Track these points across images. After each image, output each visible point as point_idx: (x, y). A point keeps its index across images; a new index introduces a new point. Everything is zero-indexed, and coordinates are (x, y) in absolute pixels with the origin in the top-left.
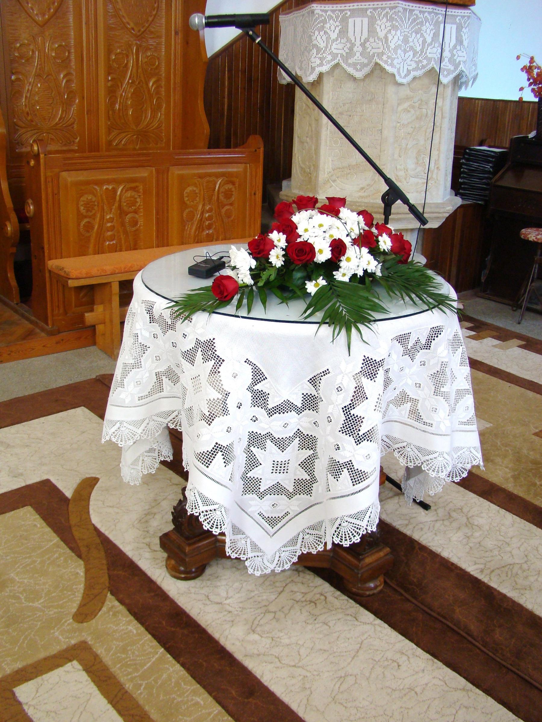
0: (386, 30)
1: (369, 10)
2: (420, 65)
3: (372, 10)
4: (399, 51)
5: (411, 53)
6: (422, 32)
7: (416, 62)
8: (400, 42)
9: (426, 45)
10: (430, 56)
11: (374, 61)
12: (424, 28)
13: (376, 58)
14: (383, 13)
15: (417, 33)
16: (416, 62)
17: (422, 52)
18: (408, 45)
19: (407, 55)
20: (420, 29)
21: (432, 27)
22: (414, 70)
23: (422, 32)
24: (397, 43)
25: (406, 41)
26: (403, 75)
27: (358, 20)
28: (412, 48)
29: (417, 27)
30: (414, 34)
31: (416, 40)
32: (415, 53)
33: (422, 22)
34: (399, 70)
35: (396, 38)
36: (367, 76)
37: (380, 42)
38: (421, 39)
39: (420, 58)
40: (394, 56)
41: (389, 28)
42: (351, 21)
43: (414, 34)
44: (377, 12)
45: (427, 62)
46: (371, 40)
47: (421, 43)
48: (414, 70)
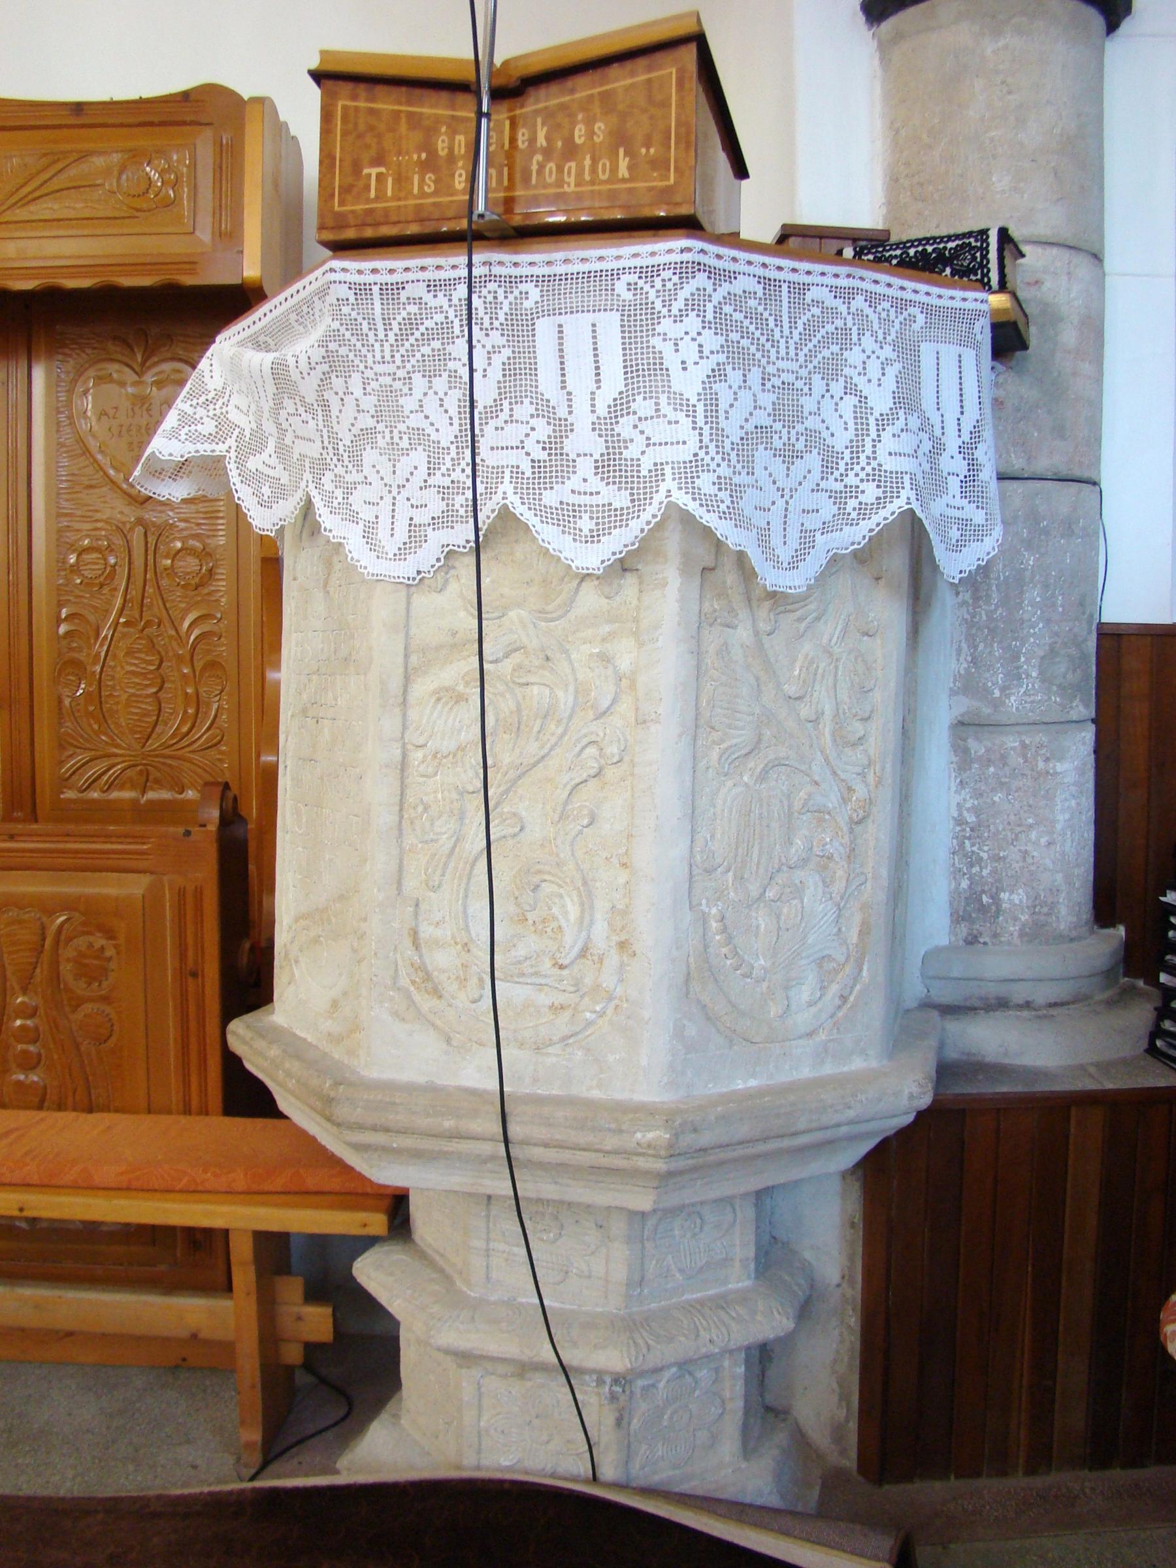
0: (706, 366)
1: (626, 278)
2: (852, 503)
3: (633, 278)
4: (762, 456)
5: (813, 460)
6: (847, 371)
8: (762, 418)
9: (872, 421)
11: (660, 497)
12: (854, 356)
13: (669, 483)
14: (683, 294)
16: (833, 495)
17: (855, 458)
18: (800, 428)
19: (799, 467)
21: (888, 352)
23: (847, 371)
24: (753, 422)
25: (787, 411)
26: (785, 554)
27: (577, 326)
32: (829, 464)
33: (846, 331)
34: (763, 539)
35: (745, 397)
36: (623, 566)
37: (681, 416)
38: (851, 400)
39: (851, 480)
40: (743, 479)
41: (714, 359)
42: (545, 328)
44: (658, 283)
46: (643, 407)
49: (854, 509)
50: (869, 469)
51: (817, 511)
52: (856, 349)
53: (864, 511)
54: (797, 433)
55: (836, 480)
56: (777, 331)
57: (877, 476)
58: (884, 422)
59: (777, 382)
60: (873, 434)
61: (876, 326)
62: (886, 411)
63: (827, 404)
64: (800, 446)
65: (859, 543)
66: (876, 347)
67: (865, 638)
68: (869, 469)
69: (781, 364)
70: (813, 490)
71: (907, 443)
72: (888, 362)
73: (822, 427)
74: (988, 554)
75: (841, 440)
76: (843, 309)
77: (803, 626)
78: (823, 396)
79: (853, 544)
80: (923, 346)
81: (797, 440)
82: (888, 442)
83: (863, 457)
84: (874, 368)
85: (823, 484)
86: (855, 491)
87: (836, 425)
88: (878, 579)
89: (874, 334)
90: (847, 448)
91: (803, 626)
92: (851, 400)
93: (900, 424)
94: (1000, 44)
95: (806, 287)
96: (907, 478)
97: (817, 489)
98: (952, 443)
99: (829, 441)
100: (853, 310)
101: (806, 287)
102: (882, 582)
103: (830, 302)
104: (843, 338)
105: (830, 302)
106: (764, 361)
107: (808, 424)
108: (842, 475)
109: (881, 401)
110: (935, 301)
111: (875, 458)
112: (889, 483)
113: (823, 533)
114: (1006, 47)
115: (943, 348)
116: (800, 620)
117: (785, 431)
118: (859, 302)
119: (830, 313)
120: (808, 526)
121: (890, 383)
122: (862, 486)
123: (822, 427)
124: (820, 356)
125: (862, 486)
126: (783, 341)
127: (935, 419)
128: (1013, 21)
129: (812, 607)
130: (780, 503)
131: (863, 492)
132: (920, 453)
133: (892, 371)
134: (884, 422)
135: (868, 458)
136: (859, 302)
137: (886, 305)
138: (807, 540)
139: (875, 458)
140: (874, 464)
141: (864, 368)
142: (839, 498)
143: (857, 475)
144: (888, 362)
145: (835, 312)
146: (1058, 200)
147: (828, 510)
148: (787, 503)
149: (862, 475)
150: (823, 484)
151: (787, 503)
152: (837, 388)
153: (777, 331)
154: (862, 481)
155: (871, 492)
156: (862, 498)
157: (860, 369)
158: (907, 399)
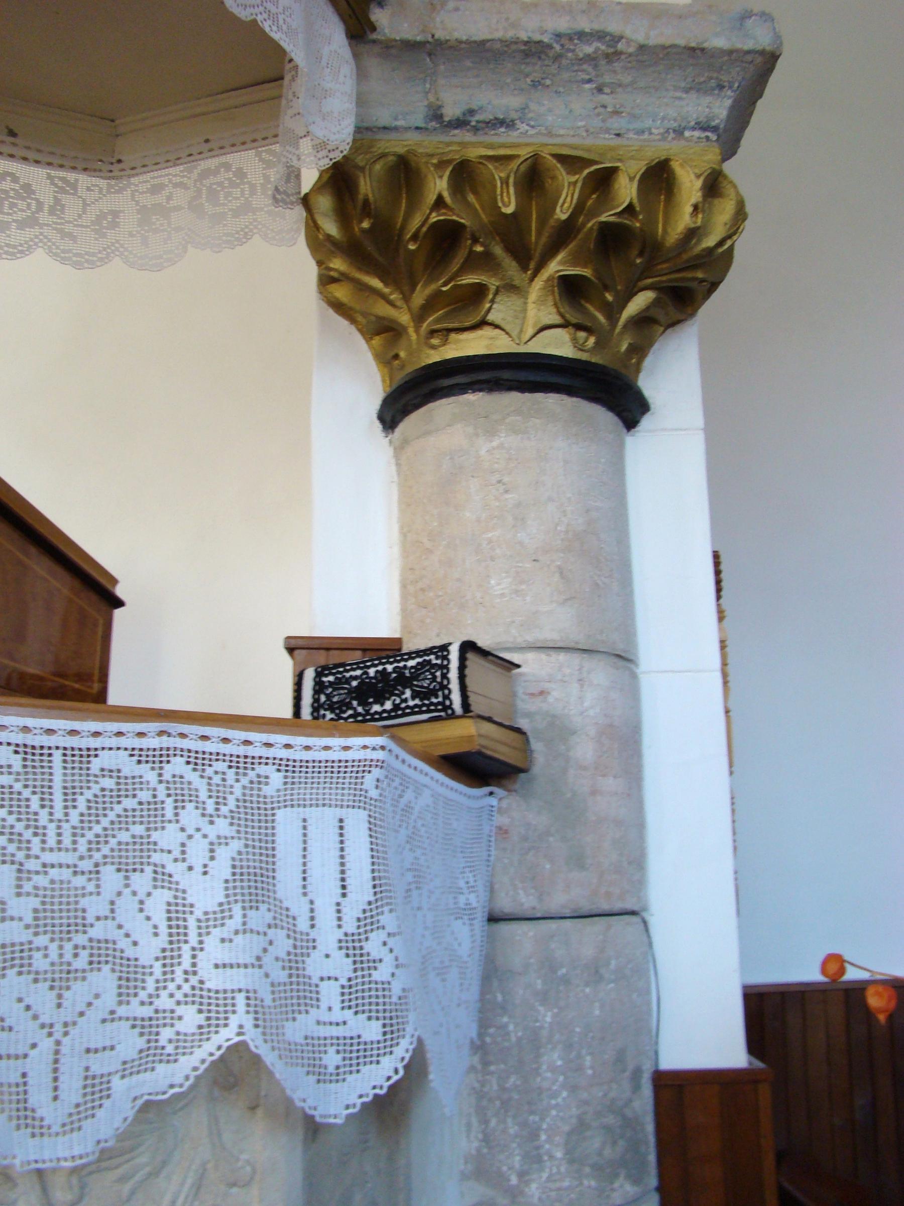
2: (166, 1034)
5: (105, 981)
7: (135, 1023)
9: (192, 923)
10: (215, 980)
12: (168, 837)
15: (126, 870)
16: (135, 1023)
20: (145, 845)
22: (127, 1069)
23: (156, 858)
28: (102, 954)
29: (124, 836)
30: (109, 874)
31: (127, 906)
33: (155, 805)
38: (163, 896)
39: (164, 1002)
43: (109, 874)
45: (201, 1019)
47: (159, 917)
48: (127, 1069)
49: (170, 1041)
50: (186, 988)
51: (112, 1048)
52: (171, 828)
53: (183, 1044)
54: (76, 947)
55: (142, 1003)
56: (44, 815)
57: (200, 996)
58: (206, 924)
59: (42, 881)
60: (193, 939)
61: (203, 795)
62: (212, 906)
63: (127, 904)
64: (81, 963)
65: (181, 1086)
66: (203, 823)
67: (235, 1190)
68: (186, 988)
69: (48, 857)
70: (104, 1021)
71: (244, 948)
72: (223, 840)
73: (118, 934)
74: (389, 1078)
75: (148, 949)
76: (151, 777)
77: (127, 1188)
78: (119, 894)
79: (172, 1086)
80: (280, 814)
81: (76, 955)
82: (214, 950)
83: (179, 971)
84: (197, 852)
85: (122, 1011)
86: (173, 1017)
87: (139, 929)
88: (253, 1108)
89: (200, 806)
90: (157, 959)
91: (127, 1188)
92: (163, 896)
93: (235, 922)
94: (495, 444)
95: (91, 753)
96: (240, 999)
97: (112, 1017)
98: (328, 936)
99: (130, 952)
100: (167, 776)
101: (91, 753)
102: (260, 1112)
103: (129, 767)
104: (152, 815)
105: (129, 767)
106: (20, 856)
107: (93, 933)
108: (150, 996)
109: (205, 893)
110: (298, 755)
111: (195, 973)
112: (214, 1007)
113: (123, 1077)
114: (501, 446)
115: (312, 813)
116: (123, 1179)
117: (54, 947)
118: (178, 765)
119: (126, 786)
120: (96, 1069)
121: (222, 868)
122: (180, 1010)
123: (118, 934)
124: (113, 842)
125: (180, 1010)
126: (52, 826)
127: (300, 908)
128: (507, 421)
129: (143, 1159)
130: (47, 1044)
131: (180, 1018)
132: (267, 960)
133: (225, 854)
134: (206, 924)
135: (186, 972)
136: (178, 765)
137: (221, 766)
138: (96, 1088)
139: (195, 973)
140: (194, 980)
141: (183, 852)
142: (147, 1027)
143: (172, 995)
144: (223, 840)
145: (138, 781)
146: (566, 600)
147: (130, 1043)
148: (58, 1043)
149: (179, 996)
150: (122, 1011)
151: (58, 1043)
152: (142, 881)
153: (44, 815)
154: (178, 1003)
155: (191, 1019)
156: (180, 1026)
157: (176, 853)
158: (254, 882)
